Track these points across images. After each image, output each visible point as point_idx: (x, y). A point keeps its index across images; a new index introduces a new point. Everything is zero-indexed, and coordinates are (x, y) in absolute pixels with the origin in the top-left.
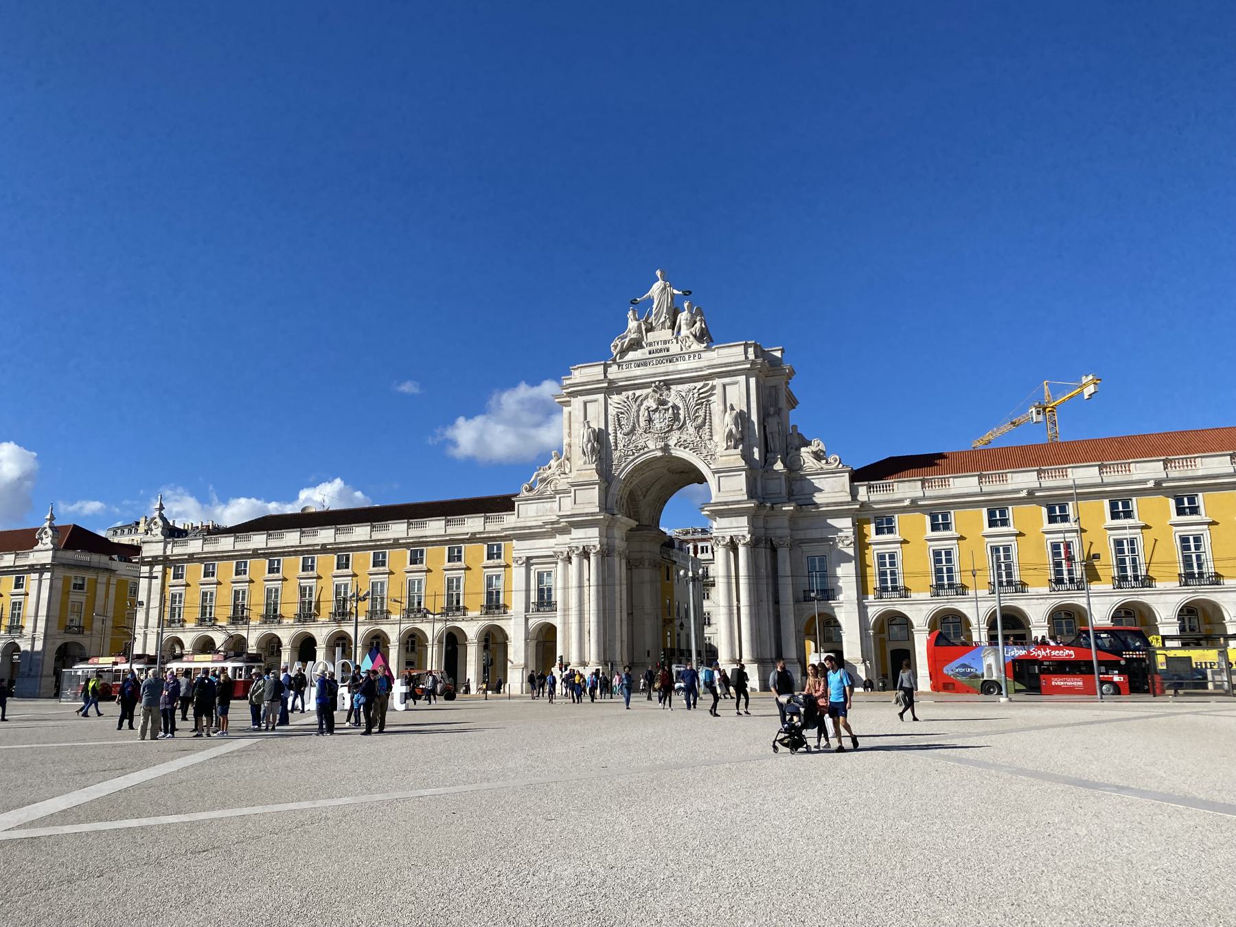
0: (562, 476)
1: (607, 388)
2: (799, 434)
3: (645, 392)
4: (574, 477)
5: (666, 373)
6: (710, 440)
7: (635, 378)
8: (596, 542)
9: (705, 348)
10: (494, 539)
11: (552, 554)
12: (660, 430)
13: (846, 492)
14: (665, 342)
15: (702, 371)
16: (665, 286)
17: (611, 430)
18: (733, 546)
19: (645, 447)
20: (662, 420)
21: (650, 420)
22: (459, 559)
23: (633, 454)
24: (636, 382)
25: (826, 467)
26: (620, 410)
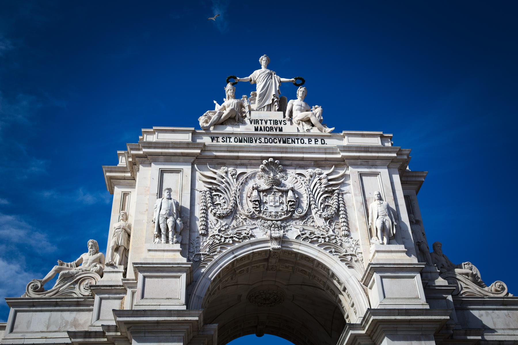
3: (249, 171)
6: (347, 236)
12: (276, 216)
14: (276, 122)
15: (333, 153)
19: (252, 236)
20: (278, 204)
21: (260, 203)
23: (233, 241)
24: (240, 154)
26: (214, 186)
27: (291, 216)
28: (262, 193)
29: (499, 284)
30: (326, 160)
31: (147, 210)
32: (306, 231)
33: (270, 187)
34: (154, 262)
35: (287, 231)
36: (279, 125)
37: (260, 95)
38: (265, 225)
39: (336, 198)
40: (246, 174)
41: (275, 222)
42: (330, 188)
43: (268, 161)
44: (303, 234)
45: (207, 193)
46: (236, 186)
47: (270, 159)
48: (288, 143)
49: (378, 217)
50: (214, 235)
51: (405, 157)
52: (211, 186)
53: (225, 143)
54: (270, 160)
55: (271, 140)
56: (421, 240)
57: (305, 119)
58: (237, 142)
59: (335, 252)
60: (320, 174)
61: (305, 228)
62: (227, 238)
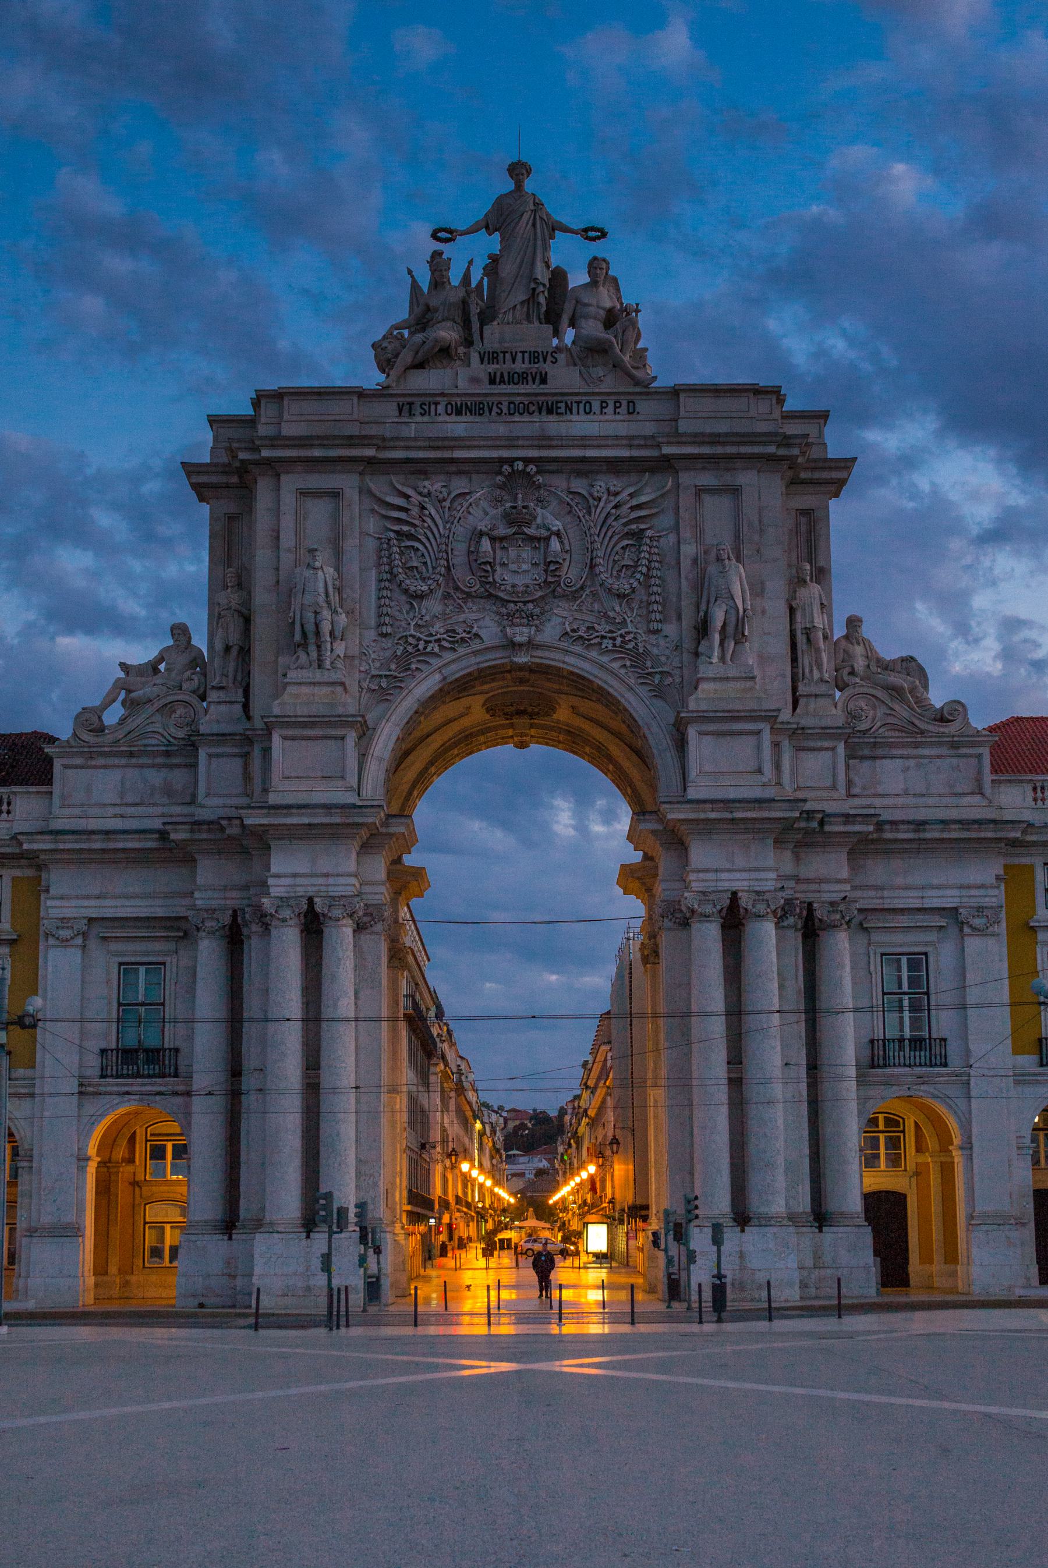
0: (213, 696)
1: (370, 461)
5: (544, 440)
6: (657, 632)
7: (457, 442)
13: (983, 795)
14: (535, 357)
23: (442, 647)
24: (458, 454)
26: (406, 528)
27: (554, 591)
30: (632, 459)
31: (278, 582)
34: (299, 713)
38: (504, 611)
39: (645, 548)
40: (468, 497)
41: (521, 604)
42: (634, 527)
43: (512, 466)
45: (391, 543)
46: (448, 526)
47: (516, 464)
48: (557, 414)
50: (406, 636)
51: (796, 451)
52: (396, 528)
53: (426, 419)
55: (521, 405)
56: (813, 622)
58: (449, 415)
59: (632, 666)
60: (616, 494)
61: (578, 616)
62: (430, 642)
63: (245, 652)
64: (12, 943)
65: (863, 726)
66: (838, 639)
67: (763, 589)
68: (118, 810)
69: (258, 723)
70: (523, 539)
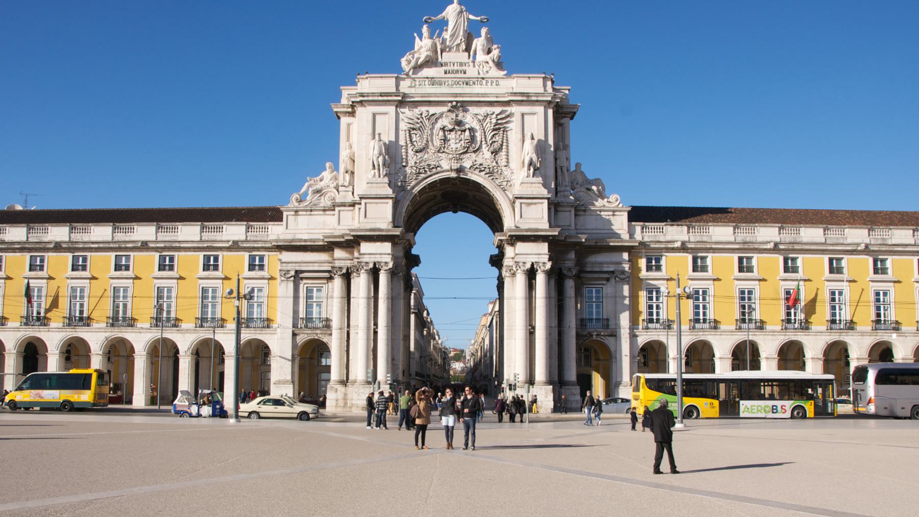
2: (581, 172)
4: (361, 188)
6: (506, 166)
8: (388, 259)
9: (504, 75)
10: (258, 249)
11: (330, 269)
12: (456, 151)
14: (461, 64)
16: (462, 9)
17: (402, 142)
18: (531, 274)
19: (438, 166)
20: (458, 141)
21: (445, 140)
22: (216, 268)
25: (607, 204)
26: (412, 126)
28: (446, 132)
29: (614, 197)
32: (477, 163)
33: (452, 127)
35: (463, 162)
36: (464, 68)
37: (451, 36)
42: (497, 127)
44: (474, 165)
45: (407, 132)
49: (528, 154)
50: (412, 167)
51: (558, 100)
53: (421, 86)
54: (454, 103)
57: (485, 61)
59: (496, 179)
61: (476, 159)
63: (353, 173)
64: (269, 279)
65: (582, 203)
66: (573, 171)
67: (545, 150)
68: (307, 231)
69: (357, 199)
70: (456, 131)
